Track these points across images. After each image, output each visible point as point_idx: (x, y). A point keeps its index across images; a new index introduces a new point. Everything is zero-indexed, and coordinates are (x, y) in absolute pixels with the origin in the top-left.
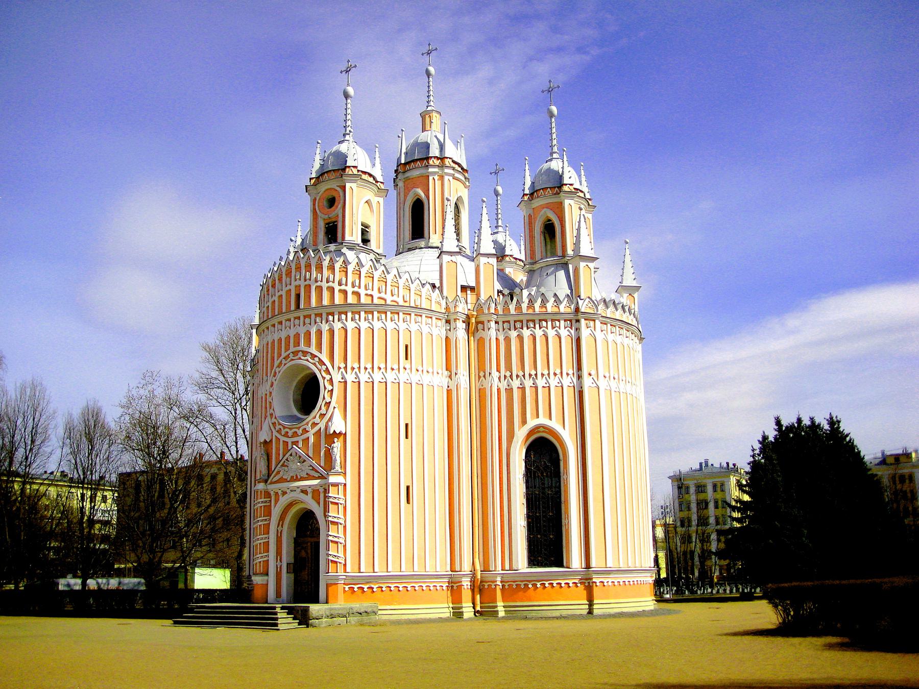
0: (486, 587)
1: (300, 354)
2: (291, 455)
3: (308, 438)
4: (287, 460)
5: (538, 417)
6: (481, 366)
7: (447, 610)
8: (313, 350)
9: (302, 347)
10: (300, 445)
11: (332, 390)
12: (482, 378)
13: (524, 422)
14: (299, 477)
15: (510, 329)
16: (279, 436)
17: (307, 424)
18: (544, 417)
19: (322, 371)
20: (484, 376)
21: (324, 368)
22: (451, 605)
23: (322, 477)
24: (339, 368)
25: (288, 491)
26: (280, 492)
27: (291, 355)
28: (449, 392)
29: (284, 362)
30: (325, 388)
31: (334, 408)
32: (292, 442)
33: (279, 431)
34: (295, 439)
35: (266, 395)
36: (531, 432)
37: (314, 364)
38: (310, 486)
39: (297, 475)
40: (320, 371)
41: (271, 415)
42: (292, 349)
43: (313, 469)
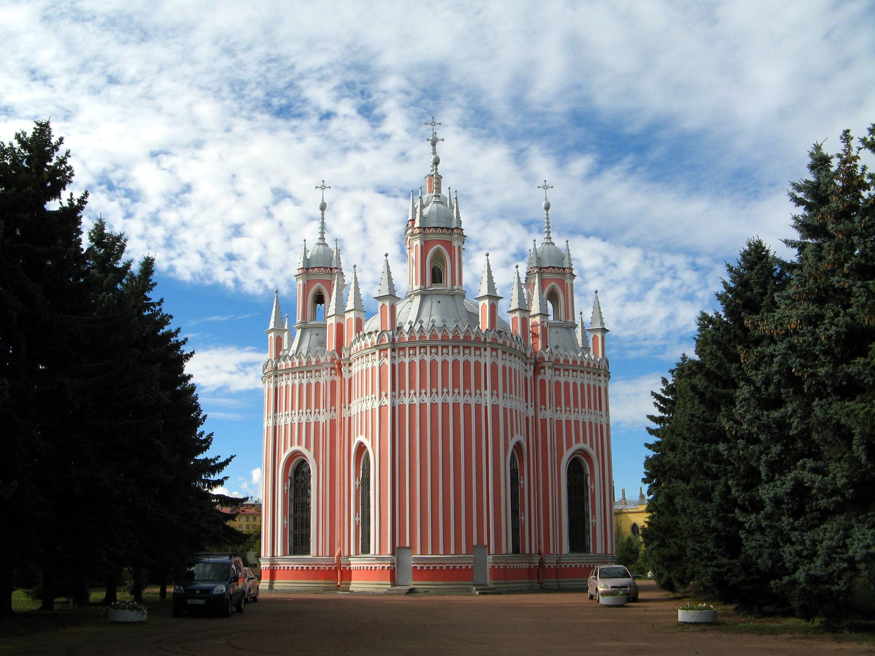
0: (547, 567)
6: (543, 402)
7: (528, 585)
13: (569, 445)
20: (545, 409)
22: (528, 581)
28: (527, 419)
36: (574, 454)
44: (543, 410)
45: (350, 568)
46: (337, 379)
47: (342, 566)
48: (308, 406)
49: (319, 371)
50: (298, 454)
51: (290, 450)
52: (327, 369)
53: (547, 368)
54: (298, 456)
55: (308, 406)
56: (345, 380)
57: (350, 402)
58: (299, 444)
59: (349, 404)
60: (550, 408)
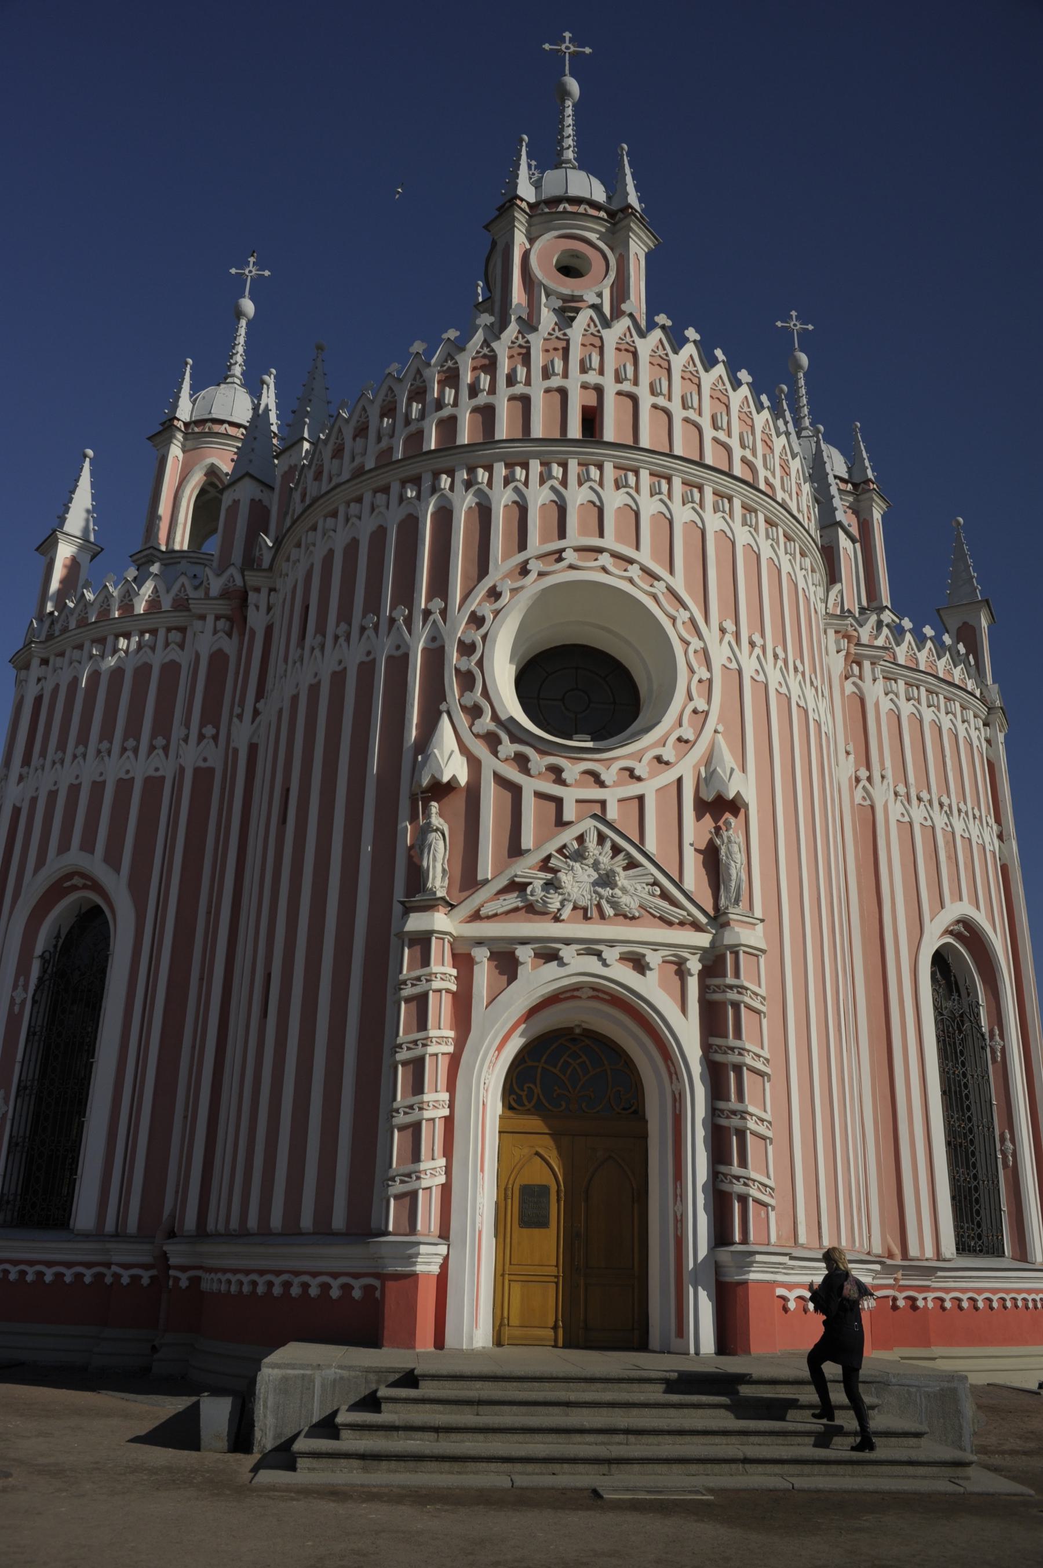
1: (605, 559)
2: (581, 839)
3: (641, 799)
4: (560, 851)
5: (961, 899)
8: (644, 556)
9: (609, 541)
10: (612, 814)
11: (710, 681)
12: (864, 782)
14: (609, 911)
15: (897, 695)
16: (513, 774)
17: (639, 756)
18: (970, 903)
19: (679, 622)
20: (869, 779)
21: (683, 616)
23: (697, 927)
24: (723, 631)
25: (567, 952)
26: (524, 954)
27: (570, 556)
29: (535, 566)
30: (692, 671)
31: (716, 731)
32: (578, 801)
33: (521, 762)
34: (596, 793)
35: (436, 656)
37: (655, 597)
38: (655, 946)
39: (599, 906)
40: (674, 620)
41: (475, 712)
42: (575, 536)
43: (665, 895)
44: (864, 782)
45: (195, 1281)
46: (229, 646)
47: (172, 1272)
48: (133, 730)
49: (183, 630)
50: (77, 881)
51: (56, 866)
52: (203, 618)
53: (867, 664)
54: (75, 888)
55: (133, 730)
56: (253, 633)
57: (260, 694)
58: (88, 846)
59: (257, 700)
60: (883, 777)
